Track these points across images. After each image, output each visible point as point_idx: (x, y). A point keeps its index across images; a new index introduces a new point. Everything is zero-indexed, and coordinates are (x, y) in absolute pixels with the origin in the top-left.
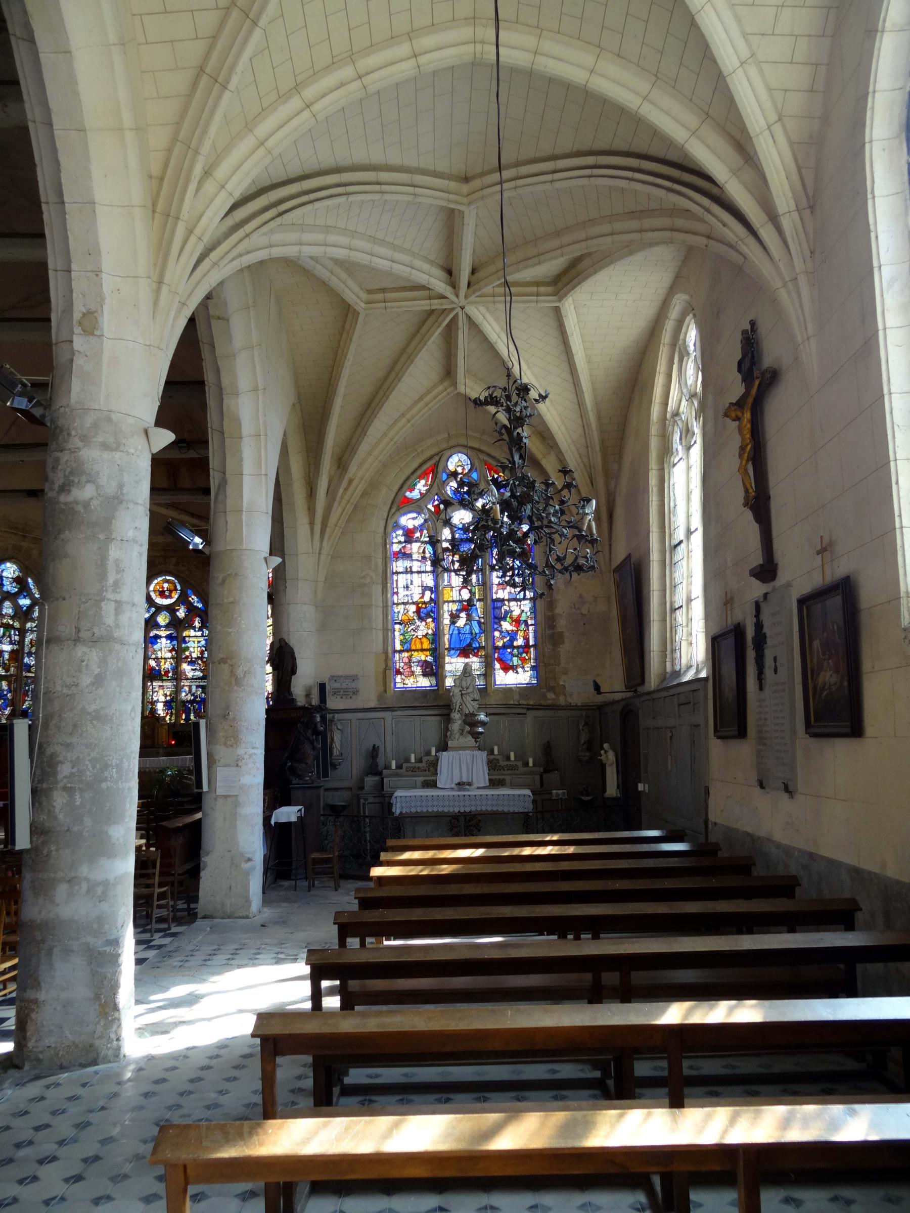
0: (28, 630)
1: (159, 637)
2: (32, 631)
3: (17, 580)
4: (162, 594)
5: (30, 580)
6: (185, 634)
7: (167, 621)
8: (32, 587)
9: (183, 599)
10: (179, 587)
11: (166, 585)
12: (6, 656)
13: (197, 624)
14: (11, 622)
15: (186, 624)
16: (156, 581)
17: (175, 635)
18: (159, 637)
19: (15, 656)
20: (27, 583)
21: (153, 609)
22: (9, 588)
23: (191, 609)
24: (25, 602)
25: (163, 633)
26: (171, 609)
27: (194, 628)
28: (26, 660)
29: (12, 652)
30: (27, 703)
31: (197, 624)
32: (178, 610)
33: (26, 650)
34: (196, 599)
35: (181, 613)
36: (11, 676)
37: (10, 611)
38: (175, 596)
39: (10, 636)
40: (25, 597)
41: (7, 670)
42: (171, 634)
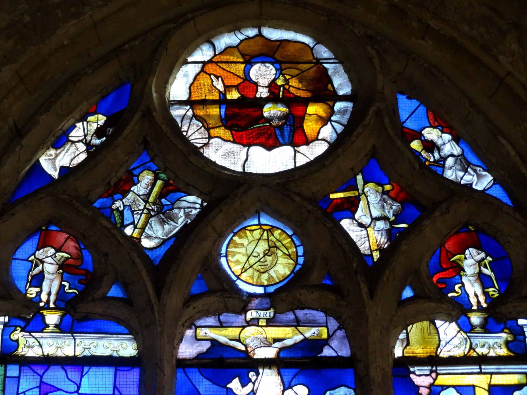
1: (244, 365)
4: (243, 120)
6: (410, 342)
7: (282, 268)
9: (373, 147)
10: (341, 83)
11: (263, 74)
13: (472, 277)
15: (413, 280)
16: (204, 53)
17: (338, 348)
18: (244, 365)
21: (192, 203)
23: (423, 197)
25: (260, 337)
26: (306, 204)
27: (459, 310)
31: (472, 277)
32: (350, 207)
34: (450, 147)
35: (367, 228)
38: (323, 134)
42: (318, 344)
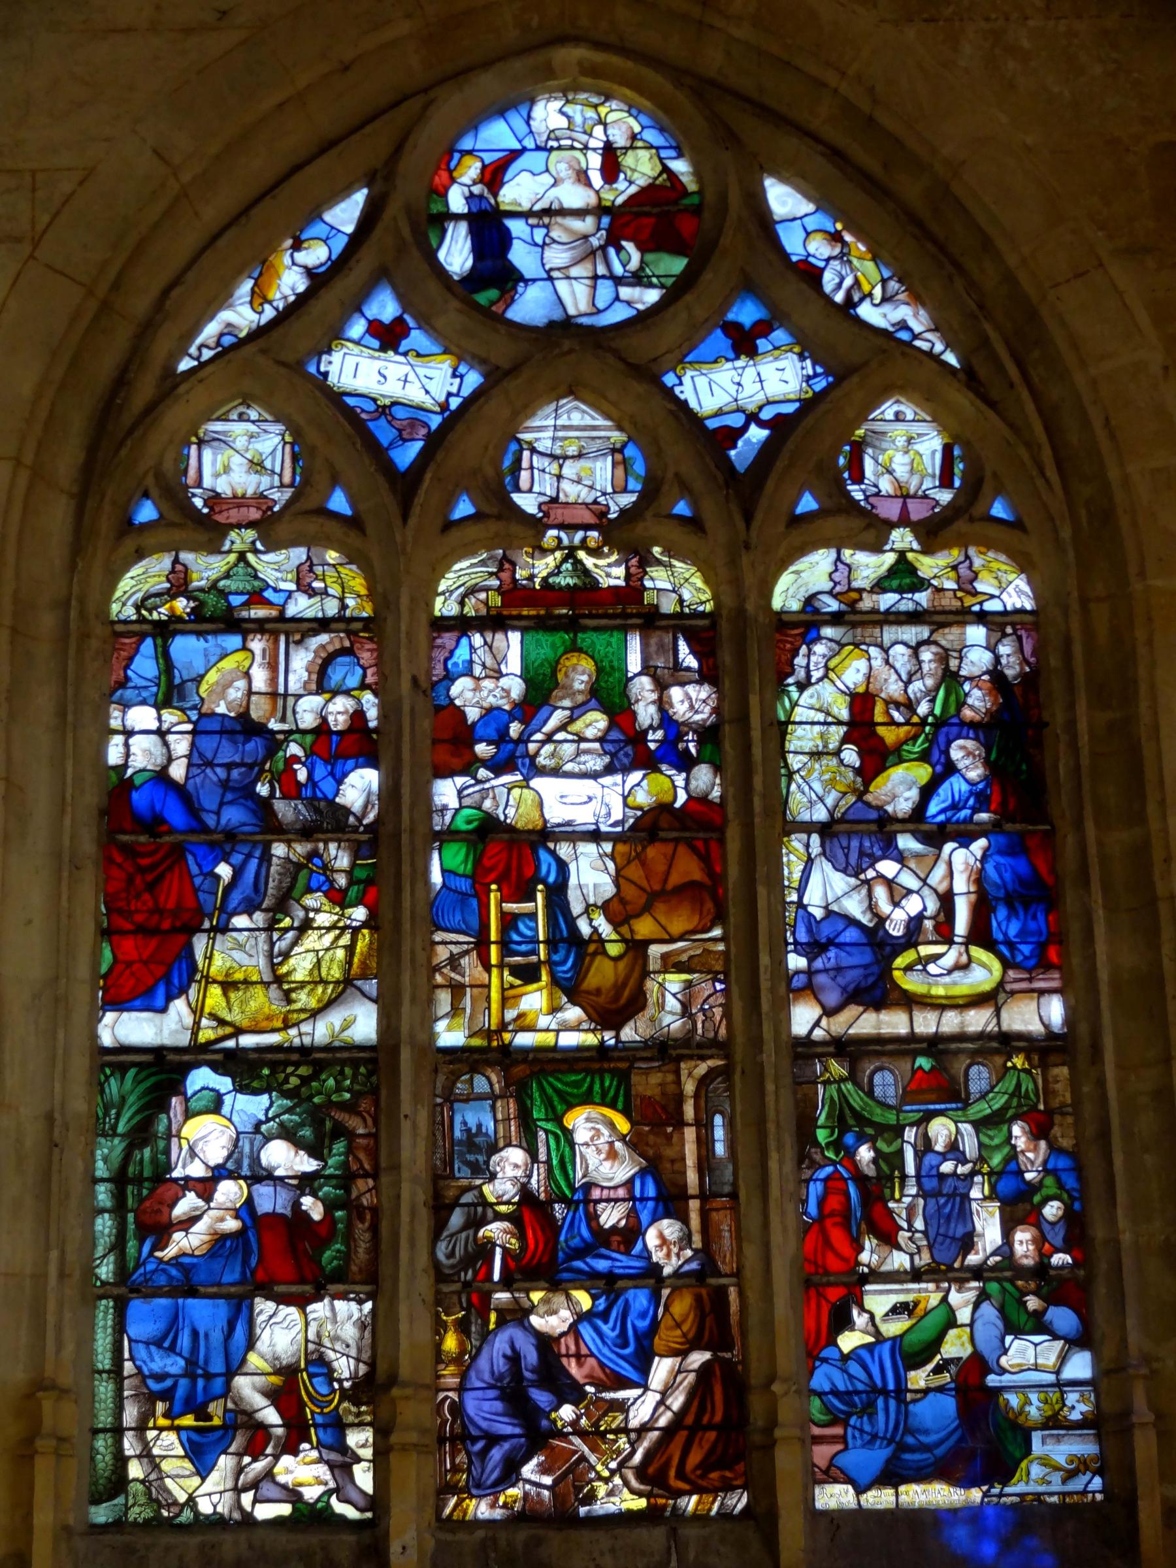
0: (808, 622)
2: (855, 618)
3: (646, 219)
5: (782, 199)
8: (820, 249)
12: (590, 875)
14: (610, 572)
19: (688, 868)
20: (764, 224)
22: (575, 297)
24: (744, 386)
28: (826, 888)
29: (649, 828)
30: (879, 1300)
33: (812, 795)
36: (665, 1051)
37: (595, 480)
39: (610, 696)
40: (744, 344)
41: (611, 1011)
